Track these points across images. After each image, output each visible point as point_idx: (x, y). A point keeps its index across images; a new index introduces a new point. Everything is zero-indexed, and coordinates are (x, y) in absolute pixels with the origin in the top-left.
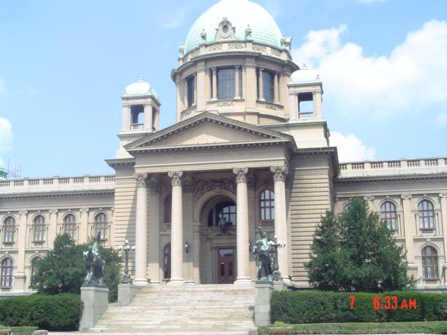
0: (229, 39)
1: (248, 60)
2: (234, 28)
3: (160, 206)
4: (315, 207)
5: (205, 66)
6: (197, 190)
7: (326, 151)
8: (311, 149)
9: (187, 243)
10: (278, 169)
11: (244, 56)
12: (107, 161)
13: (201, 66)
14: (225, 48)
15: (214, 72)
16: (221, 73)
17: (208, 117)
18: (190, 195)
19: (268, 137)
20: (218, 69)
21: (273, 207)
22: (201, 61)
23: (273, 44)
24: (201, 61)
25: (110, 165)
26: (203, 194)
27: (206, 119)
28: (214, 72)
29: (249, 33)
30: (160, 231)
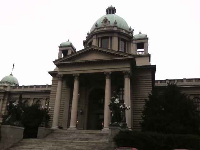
0: (107, 26)
1: (114, 34)
2: (109, 22)
5: (96, 36)
10: (127, 72)
11: (113, 32)
12: (48, 72)
13: (95, 37)
14: (105, 29)
15: (100, 39)
16: (103, 40)
17: (93, 48)
19: (122, 56)
20: (102, 38)
21: (124, 94)
22: (94, 35)
23: (126, 29)
24: (94, 35)
28: (100, 39)
29: (116, 23)
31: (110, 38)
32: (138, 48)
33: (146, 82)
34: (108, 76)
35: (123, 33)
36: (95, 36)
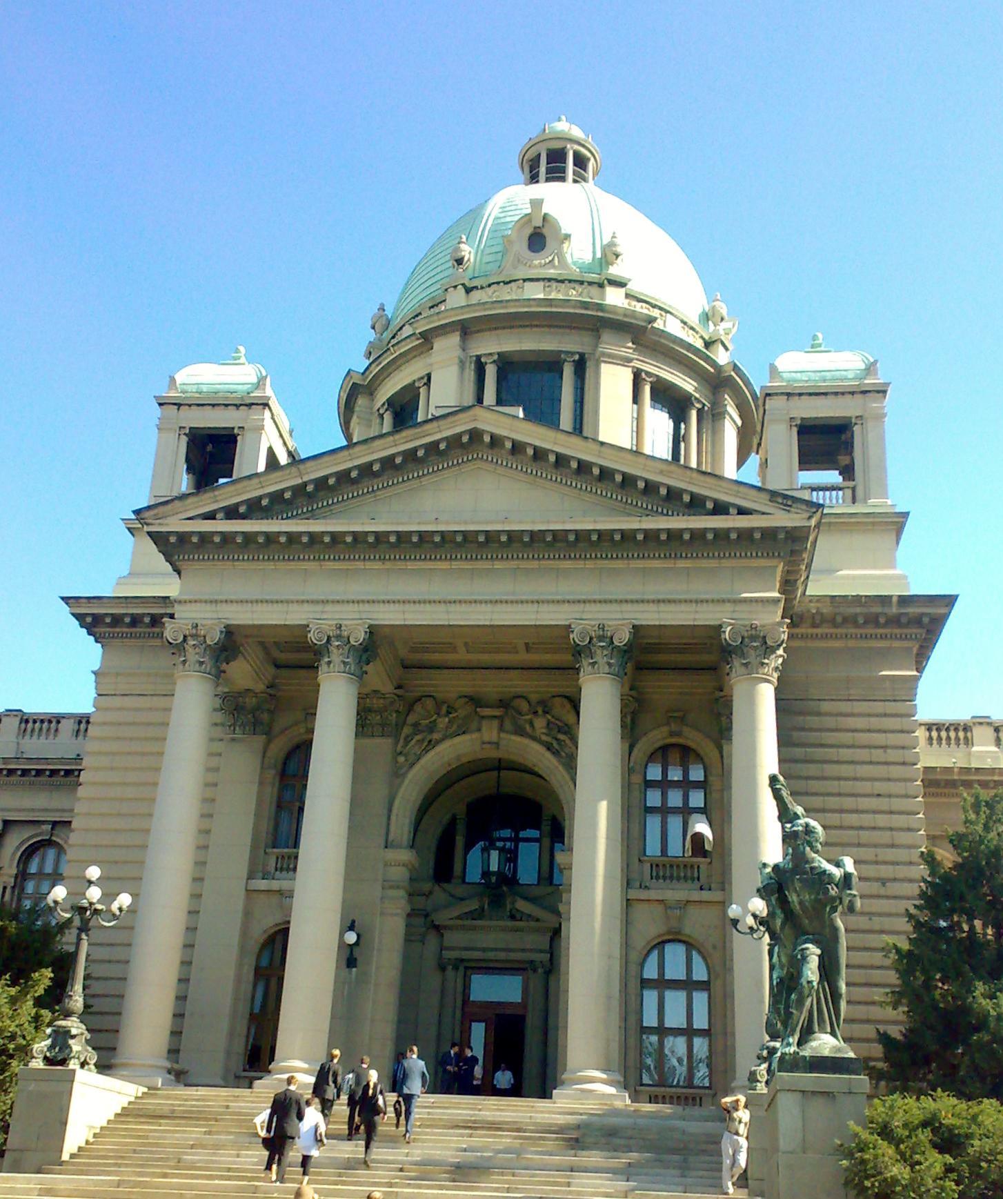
1: (606, 336)
3: (261, 783)
4: (867, 819)
6: (406, 730)
7: (912, 610)
8: (858, 598)
9: (351, 928)
13: (448, 346)
15: (491, 373)
18: (382, 745)
19: (720, 509)
22: (443, 330)
24: (443, 330)
26: (431, 744)
27: (475, 435)
30: (251, 876)
31: (568, 371)
32: (807, 460)
33: (875, 722)
34: (601, 657)
35: (662, 333)
36: (455, 339)
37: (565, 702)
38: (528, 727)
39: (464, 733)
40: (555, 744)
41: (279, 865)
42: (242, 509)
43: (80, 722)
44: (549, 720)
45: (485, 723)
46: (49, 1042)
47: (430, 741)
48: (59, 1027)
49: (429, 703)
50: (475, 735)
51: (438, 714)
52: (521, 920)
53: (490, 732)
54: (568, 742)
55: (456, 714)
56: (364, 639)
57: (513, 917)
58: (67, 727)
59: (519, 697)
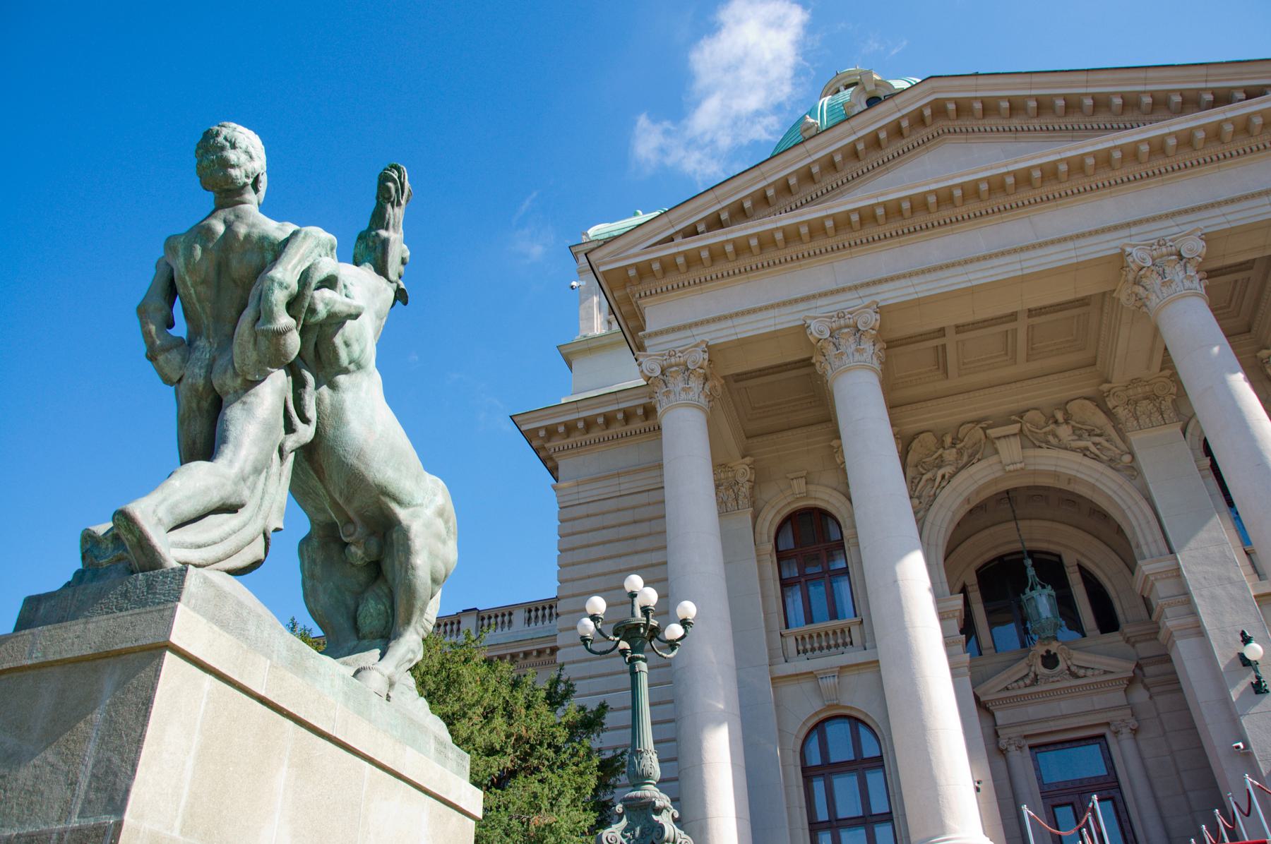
25: (529, 436)
37: (1087, 402)
38: (1050, 438)
39: (979, 460)
40: (1093, 449)
41: (801, 648)
42: (701, 228)
43: (530, 611)
44: (1073, 427)
45: (1001, 445)
46: (624, 822)
47: (943, 477)
48: (631, 799)
49: (929, 439)
50: (994, 459)
51: (944, 448)
52: (1085, 676)
53: (1010, 451)
54: (1106, 444)
55: (962, 445)
56: (876, 320)
57: (1075, 676)
58: (519, 617)
59: (1028, 411)
